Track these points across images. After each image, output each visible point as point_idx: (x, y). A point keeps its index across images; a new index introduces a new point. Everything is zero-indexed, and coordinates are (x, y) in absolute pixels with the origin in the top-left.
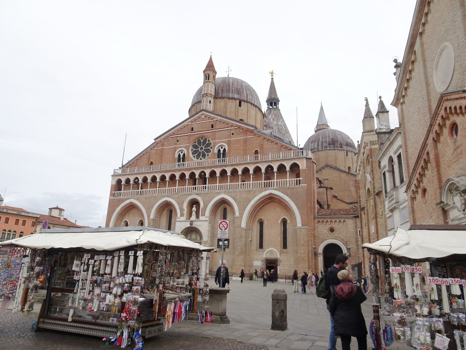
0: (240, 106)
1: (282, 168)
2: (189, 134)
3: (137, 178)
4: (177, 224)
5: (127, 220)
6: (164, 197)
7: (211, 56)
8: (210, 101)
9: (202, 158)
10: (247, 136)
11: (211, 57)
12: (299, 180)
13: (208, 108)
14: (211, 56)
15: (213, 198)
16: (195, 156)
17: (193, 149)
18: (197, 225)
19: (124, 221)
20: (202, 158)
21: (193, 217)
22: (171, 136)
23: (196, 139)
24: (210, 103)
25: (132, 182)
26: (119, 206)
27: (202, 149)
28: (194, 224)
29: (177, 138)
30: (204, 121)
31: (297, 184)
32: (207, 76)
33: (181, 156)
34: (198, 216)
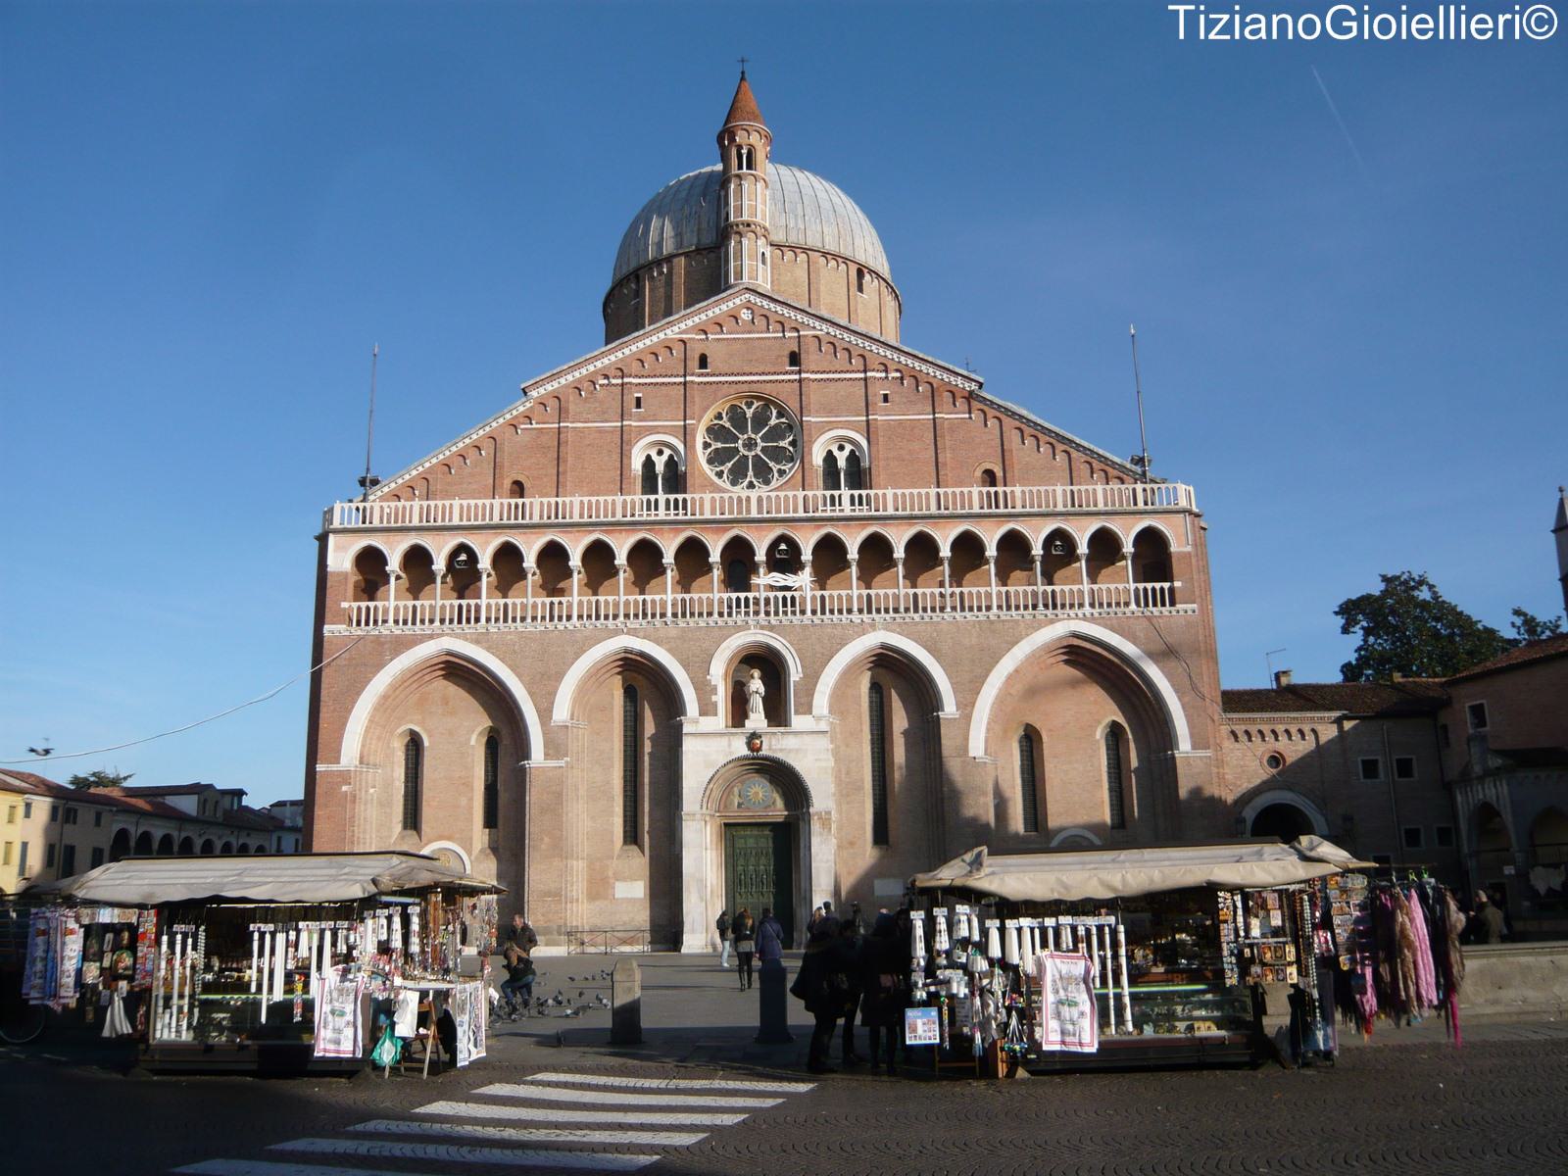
0: (860, 289)
1: (1105, 546)
2: (688, 378)
3: (463, 548)
4: (689, 746)
5: (417, 729)
6: (617, 632)
7: (743, 73)
8: (763, 254)
9: (753, 480)
10: (946, 414)
11: (743, 79)
12: (1172, 590)
13: (760, 281)
14: (743, 73)
15: (842, 644)
16: (722, 472)
17: (708, 440)
18: (781, 750)
19: (404, 728)
20: (755, 483)
21: (757, 720)
22: (606, 382)
23: (723, 403)
24: (764, 262)
25: (439, 565)
26: (380, 666)
27: (750, 444)
28: (764, 747)
29: (631, 394)
30: (754, 332)
31: (1163, 605)
32: (744, 151)
33: (660, 468)
34: (777, 713)
